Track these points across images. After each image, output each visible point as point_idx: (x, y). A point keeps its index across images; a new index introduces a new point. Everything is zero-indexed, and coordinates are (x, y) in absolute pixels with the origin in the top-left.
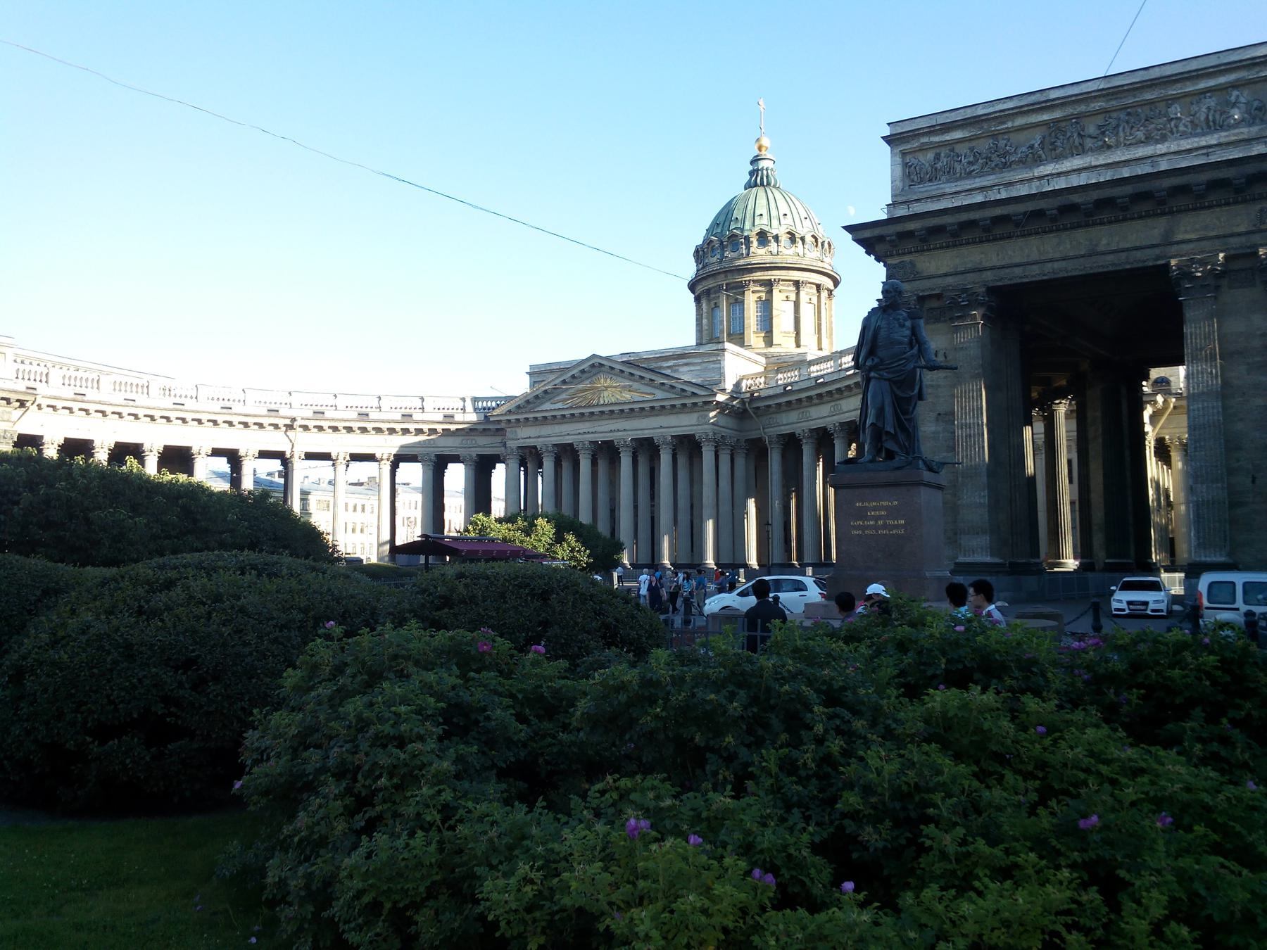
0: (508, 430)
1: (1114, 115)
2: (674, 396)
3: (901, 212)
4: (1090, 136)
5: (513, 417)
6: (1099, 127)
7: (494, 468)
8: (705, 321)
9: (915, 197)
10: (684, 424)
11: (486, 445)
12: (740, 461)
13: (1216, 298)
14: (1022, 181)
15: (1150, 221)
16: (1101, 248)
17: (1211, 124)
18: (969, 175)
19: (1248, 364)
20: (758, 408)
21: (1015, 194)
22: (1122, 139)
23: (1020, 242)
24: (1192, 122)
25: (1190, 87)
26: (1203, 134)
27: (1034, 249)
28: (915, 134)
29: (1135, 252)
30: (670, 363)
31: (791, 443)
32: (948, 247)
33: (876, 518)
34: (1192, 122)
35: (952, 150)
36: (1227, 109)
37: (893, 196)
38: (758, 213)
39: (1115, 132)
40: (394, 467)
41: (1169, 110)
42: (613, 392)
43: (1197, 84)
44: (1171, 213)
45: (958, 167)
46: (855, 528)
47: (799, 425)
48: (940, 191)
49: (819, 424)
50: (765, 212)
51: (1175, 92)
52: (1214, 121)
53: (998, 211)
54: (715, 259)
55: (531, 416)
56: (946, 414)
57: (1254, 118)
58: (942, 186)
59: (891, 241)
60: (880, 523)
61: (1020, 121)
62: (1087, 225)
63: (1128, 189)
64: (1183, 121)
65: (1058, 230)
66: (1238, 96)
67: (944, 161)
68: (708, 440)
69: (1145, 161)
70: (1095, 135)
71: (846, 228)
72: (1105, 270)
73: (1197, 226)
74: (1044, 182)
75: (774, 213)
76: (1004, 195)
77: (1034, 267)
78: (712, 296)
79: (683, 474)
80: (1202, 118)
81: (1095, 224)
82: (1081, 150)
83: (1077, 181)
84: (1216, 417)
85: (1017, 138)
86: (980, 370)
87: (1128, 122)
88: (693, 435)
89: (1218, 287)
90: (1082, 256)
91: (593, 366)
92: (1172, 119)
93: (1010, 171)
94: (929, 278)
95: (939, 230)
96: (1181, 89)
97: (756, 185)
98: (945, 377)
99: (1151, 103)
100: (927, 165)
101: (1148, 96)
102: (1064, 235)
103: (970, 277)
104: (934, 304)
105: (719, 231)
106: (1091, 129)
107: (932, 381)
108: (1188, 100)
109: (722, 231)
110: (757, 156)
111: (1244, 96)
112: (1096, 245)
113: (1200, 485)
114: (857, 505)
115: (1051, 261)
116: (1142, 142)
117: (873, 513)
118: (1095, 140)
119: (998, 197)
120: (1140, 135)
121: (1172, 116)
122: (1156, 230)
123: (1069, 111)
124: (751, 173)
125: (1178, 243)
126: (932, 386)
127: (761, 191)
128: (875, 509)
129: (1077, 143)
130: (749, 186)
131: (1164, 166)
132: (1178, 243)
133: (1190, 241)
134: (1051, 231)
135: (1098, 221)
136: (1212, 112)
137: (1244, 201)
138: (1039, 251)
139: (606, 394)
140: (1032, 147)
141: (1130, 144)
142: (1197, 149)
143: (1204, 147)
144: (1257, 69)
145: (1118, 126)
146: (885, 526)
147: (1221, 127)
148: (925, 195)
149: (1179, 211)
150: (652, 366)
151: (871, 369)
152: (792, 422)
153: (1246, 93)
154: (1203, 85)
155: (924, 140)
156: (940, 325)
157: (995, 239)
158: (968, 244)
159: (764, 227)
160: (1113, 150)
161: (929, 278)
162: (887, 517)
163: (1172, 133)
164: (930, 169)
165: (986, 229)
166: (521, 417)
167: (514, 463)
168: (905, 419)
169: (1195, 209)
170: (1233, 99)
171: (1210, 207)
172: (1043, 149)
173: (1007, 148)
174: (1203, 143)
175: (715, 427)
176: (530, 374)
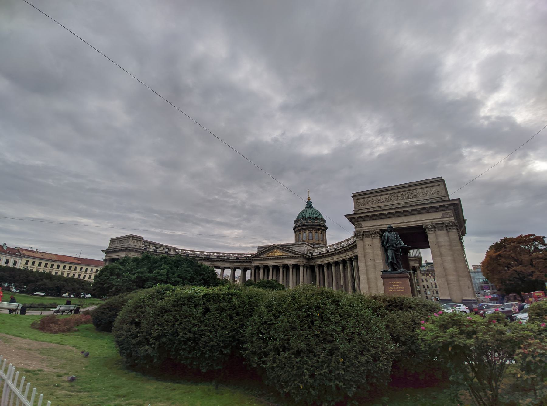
1: (404, 192)
5: (254, 259)
6: (401, 195)
11: (246, 265)
12: (308, 271)
20: (313, 258)
30: (292, 246)
31: (321, 266)
33: (396, 287)
37: (355, 208)
38: (309, 213)
40: (224, 270)
42: (278, 254)
49: (328, 262)
50: (310, 213)
60: (397, 288)
61: (383, 193)
68: (301, 265)
71: (345, 215)
75: (312, 213)
79: (295, 274)
82: (398, 199)
88: (298, 264)
91: (273, 247)
120: (411, 196)
127: (309, 209)
130: (306, 208)
139: (276, 253)
144: (436, 183)
146: (399, 289)
152: (321, 261)
165: (363, 219)
167: (253, 271)
170: (431, 189)
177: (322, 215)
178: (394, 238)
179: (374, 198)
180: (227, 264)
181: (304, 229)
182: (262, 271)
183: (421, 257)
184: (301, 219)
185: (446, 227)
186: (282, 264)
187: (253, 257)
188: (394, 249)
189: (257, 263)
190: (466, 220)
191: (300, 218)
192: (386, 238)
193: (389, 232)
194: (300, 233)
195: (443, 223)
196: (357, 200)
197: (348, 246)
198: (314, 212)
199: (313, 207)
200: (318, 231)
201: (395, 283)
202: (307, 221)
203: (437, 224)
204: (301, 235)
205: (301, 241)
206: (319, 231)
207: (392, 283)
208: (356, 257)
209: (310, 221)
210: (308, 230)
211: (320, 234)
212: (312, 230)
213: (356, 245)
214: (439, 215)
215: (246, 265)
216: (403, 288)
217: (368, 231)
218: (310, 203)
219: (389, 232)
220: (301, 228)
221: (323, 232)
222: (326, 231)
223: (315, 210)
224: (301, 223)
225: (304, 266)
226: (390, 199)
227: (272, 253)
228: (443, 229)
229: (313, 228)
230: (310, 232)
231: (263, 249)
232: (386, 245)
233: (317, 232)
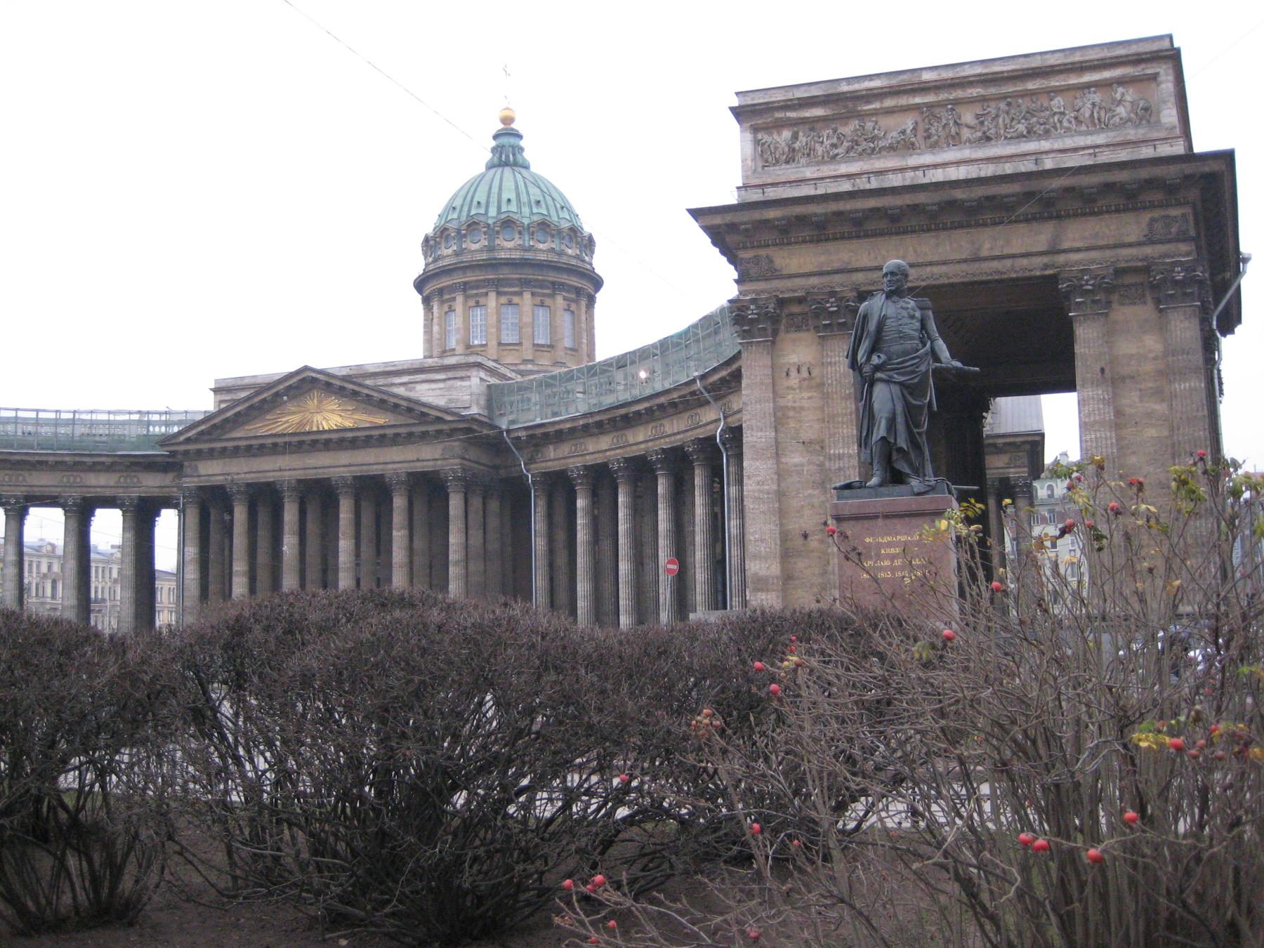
0: (186, 464)
1: (993, 104)
2: (412, 421)
3: (756, 196)
6: (977, 116)
7: (158, 515)
8: (436, 328)
9: (769, 181)
10: (427, 456)
11: (151, 483)
12: (494, 505)
13: (1106, 315)
14: (894, 171)
15: (1035, 225)
16: (985, 253)
17: (1097, 121)
19: (1140, 390)
21: (887, 185)
22: (1002, 132)
23: (894, 240)
24: (1076, 118)
25: (1073, 80)
26: (1091, 133)
27: (911, 248)
28: (768, 108)
29: (1021, 259)
30: (405, 379)
32: (811, 241)
33: (892, 558)
36: (1113, 107)
37: (745, 177)
38: (505, 196)
39: (994, 123)
41: (1052, 103)
43: (1081, 76)
44: (1059, 217)
45: (820, 149)
47: (571, 460)
48: (799, 176)
49: (599, 459)
50: (513, 196)
51: (1058, 84)
52: (1099, 120)
53: (872, 203)
54: (450, 251)
55: (218, 445)
56: (810, 443)
57: (1141, 120)
58: (802, 169)
59: (747, 230)
61: (889, 103)
62: (969, 226)
63: (1015, 188)
64: (1067, 117)
65: (937, 229)
66: (1123, 95)
67: (802, 139)
69: (1028, 157)
72: (989, 278)
73: (1087, 234)
74: (920, 173)
75: (524, 198)
76: (874, 184)
78: (446, 297)
80: (1087, 115)
81: (977, 225)
84: (1109, 450)
85: (886, 122)
86: (852, 390)
87: (1007, 113)
89: (1109, 304)
90: (965, 261)
91: (304, 380)
92: (1055, 114)
93: (879, 158)
94: (790, 276)
95: (802, 220)
96: (1064, 80)
97: (499, 165)
98: (810, 398)
99: (1032, 93)
100: (783, 144)
101: (1031, 85)
102: (943, 234)
103: (838, 278)
104: (795, 309)
105: (455, 216)
106: (968, 117)
107: (795, 402)
108: (1072, 93)
109: (459, 218)
110: (502, 129)
111: (1130, 94)
112: (979, 249)
114: (867, 540)
115: (931, 264)
116: (1024, 136)
117: (888, 551)
118: (973, 131)
119: (868, 187)
121: (1056, 110)
122: (1043, 236)
123: (943, 96)
124: (494, 150)
125: (1065, 251)
126: (794, 408)
127: (507, 170)
128: (889, 545)
130: (491, 166)
131: (1049, 164)
132: (1065, 251)
133: (1078, 250)
134: (929, 230)
135: (981, 222)
137: (1135, 209)
138: (915, 251)
139: (318, 418)
140: (903, 132)
141: (1011, 138)
142: (1083, 148)
143: (1088, 148)
144: (1143, 66)
145: (997, 116)
147: (1107, 126)
149: (1068, 216)
150: (380, 381)
151: (878, 368)
152: (555, 458)
153: (1131, 91)
154: (1088, 78)
155: (779, 115)
156: (802, 335)
157: (866, 236)
158: (835, 239)
159: (511, 215)
160: (993, 142)
161: (790, 276)
163: (1055, 127)
164: (786, 149)
166: (205, 446)
168: (918, 433)
169: (1084, 215)
170: (1118, 96)
171: (1100, 213)
173: (876, 131)
175: (466, 463)
176: (216, 391)
177: (577, 209)
178: (912, 327)
179: (849, 129)
180: (42, 481)
181: (477, 285)
182: (240, 514)
183: (1042, 435)
184: (458, 231)
185: (1154, 287)
186: (345, 472)
187: (188, 440)
188: (902, 379)
189: (212, 471)
190: (1246, 260)
191: (454, 225)
192: (872, 326)
193: (889, 295)
194: (451, 310)
195: (1146, 270)
196: (759, 136)
197: (703, 377)
198: (535, 193)
199: (527, 167)
200: (552, 296)
201: (889, 539)
202: (491, 239)
203: (1119, 272)
204: (456, 320)
205: (460, 350)
206: (559, 300)
208: (735, 434)
209: (510, 245)
210: (499, 294)
211: (560, 313)
212: (520, 294)
213: (737, 376)
214: (1131, 227)
215: (151, 483)
217: (800, 301)
218: (512, 140)
219: (889, 295)
220: (458, 279)
221: (577, 302)
222: (591, 301)
223: (537, 182)
224: (456, 254)
225: (469, 485)
226: (921, 134)
227: (295, 419)
228: (1142, 300)
229: (525, 283)
230: (510, 303)
231: (243, 395)
232: (869, 359)
233: (548, 301)
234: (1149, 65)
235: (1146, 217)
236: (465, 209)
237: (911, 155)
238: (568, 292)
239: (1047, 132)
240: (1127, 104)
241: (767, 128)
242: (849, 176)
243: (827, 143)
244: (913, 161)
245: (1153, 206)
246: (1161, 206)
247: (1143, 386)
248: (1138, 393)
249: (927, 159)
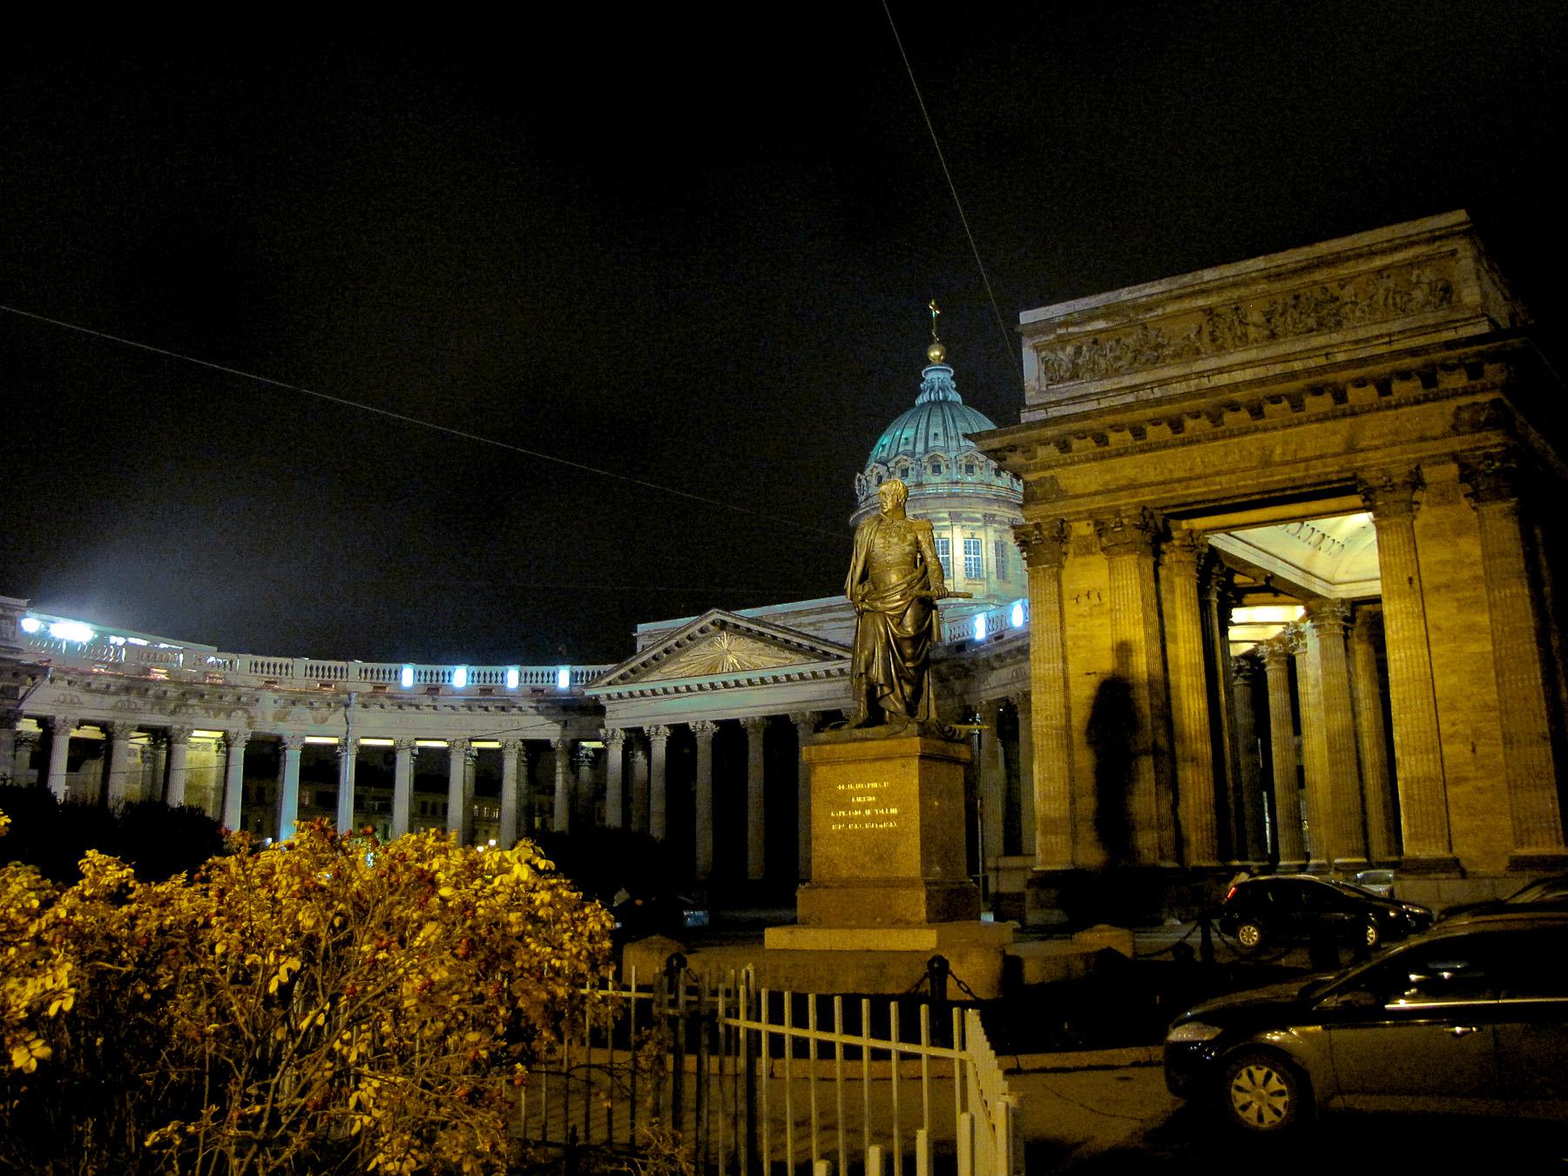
4: (1255, 325)
18: (1117, 372)
19: (1458, 600)
22: (1290, 328)
24: (1369, 306)
30: (813, 618)
32: (1094, 459)
33: (864, 807)
34: (1369, 306)
35: (1095, 342)
38: (932, 432)
45: (1102, 362)
46: (837, 820)
50: (940, 430)
52: (1395, 304)
60: (868, 812)
66: (1419, 276)
70: (1259, 322)
76: (1158, 393)
77: (1200, 482)
82: (1243, 340)
83: (1239, 376)
87: (1295, 307)
107: (1085, 630)
111: (1428, 275)
112: (1270, 456)
113: (1407, 758)
117: (859, 799)
125: (1362, 450)
126: (1084, 636)
129: (1239, 333)
133: (1377, 448)
136: (1391, 294)
138: (1203, 462)
143: (1382, 336)
144: (1438, 244)
146: (873, 818)
148: (1067, 395)
155: (1060, 331)
162: (876, 805)
170: (1414, 279)
172: (1200, 339)
174: (1384, 331)
196: (1044, 354)
207: (850, 787)
216: (894, 811)
226: (1206, 338)
234: (1444, 242)
235: (1450, 406)
236: (894, 447)
237: (1196, 361)
238: (1000, 523)
239: (1339, 324)
240: (1425, 287)
241: (1050, 347)
242: (1133, 388)
243: (1110, 355)
244: (1200, 366)
245: (1455, 393)
246: (1466, 392)
247: (1459, 595)
248: (1455, 604)
249: (1213, 363)
